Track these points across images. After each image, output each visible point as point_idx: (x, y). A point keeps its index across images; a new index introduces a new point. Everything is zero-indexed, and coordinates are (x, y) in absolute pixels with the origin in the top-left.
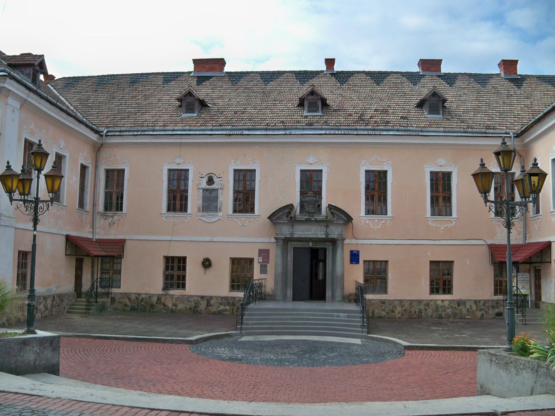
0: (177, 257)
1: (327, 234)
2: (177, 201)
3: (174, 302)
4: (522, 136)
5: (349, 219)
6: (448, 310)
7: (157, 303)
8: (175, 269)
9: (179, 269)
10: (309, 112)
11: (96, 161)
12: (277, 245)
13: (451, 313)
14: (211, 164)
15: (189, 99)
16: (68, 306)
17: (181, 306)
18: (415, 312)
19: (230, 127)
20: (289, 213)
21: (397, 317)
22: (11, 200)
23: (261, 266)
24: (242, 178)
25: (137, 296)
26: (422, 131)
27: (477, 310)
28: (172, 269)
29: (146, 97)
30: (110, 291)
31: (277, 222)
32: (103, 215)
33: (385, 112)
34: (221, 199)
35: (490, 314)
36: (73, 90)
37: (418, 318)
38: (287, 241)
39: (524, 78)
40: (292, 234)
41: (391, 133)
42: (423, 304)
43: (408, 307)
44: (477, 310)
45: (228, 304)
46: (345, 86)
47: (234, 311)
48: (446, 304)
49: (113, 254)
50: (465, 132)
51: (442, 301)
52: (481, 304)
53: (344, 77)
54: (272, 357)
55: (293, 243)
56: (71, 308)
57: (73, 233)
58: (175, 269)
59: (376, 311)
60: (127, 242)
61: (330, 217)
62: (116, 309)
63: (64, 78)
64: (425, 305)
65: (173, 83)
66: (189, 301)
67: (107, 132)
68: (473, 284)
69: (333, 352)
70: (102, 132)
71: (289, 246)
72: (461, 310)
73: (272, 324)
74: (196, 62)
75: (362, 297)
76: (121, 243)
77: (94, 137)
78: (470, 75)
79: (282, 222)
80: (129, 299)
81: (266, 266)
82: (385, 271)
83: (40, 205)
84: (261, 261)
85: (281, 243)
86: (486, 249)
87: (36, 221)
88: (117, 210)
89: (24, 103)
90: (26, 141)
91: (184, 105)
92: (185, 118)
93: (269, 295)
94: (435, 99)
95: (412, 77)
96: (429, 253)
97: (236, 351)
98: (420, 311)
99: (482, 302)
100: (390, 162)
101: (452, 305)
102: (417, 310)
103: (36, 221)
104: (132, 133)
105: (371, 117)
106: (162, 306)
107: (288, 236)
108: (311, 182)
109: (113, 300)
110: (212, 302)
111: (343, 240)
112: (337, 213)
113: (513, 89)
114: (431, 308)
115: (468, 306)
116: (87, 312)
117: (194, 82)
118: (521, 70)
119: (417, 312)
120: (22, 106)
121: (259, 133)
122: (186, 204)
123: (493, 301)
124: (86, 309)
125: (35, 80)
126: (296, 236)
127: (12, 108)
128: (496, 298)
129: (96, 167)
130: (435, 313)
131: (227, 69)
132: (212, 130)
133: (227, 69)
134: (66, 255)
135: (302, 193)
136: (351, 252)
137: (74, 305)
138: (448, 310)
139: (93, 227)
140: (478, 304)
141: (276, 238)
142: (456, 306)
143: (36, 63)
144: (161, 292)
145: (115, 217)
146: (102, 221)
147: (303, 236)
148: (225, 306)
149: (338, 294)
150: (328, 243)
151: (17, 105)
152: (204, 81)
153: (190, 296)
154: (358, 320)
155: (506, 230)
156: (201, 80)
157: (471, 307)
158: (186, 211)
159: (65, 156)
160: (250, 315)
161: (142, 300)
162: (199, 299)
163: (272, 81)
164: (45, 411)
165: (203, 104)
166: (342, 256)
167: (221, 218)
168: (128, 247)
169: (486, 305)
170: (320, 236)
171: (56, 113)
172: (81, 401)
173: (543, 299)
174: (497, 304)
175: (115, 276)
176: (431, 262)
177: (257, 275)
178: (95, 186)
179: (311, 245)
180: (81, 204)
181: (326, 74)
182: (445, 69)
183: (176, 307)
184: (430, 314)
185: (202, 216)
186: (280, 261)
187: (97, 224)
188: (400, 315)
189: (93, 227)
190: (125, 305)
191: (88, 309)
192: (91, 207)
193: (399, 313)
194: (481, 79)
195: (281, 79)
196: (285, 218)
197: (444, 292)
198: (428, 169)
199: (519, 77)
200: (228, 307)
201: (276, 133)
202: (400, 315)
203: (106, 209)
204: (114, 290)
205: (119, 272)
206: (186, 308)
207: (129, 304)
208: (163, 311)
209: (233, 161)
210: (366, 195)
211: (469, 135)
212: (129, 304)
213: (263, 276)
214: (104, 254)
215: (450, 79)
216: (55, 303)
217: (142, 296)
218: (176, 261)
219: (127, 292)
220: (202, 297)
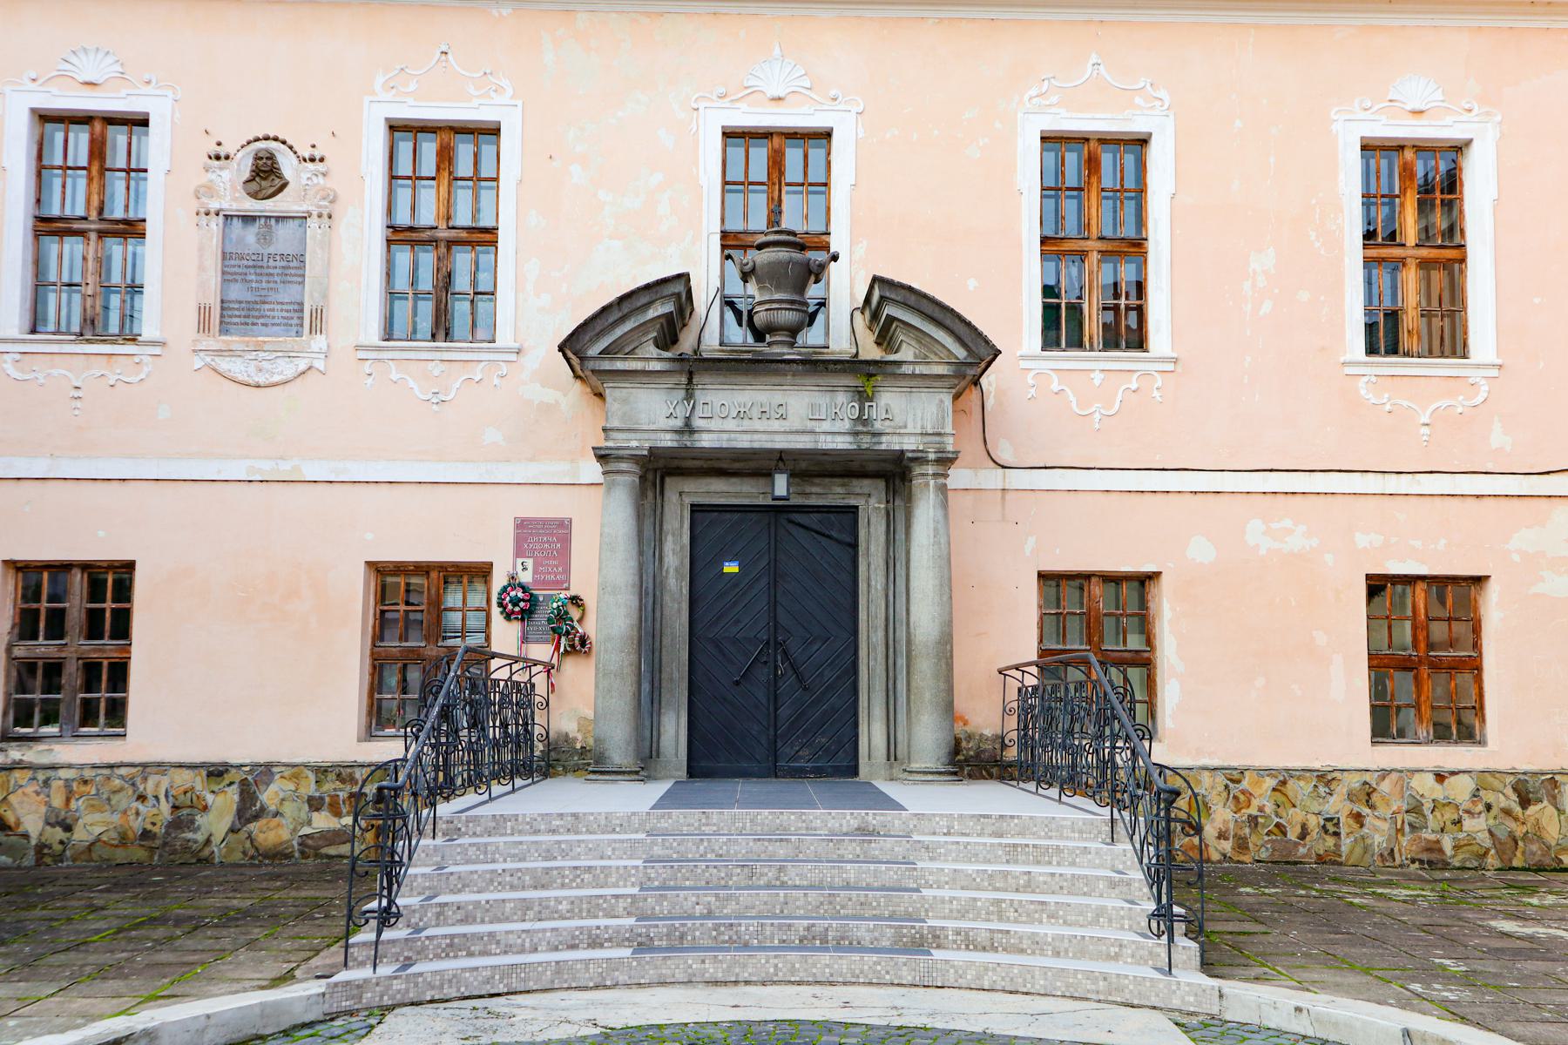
0: (86, 566)
3: (58, 801)
9: (94, 631)
17: (92, 825)
18: (1304, 834)
20: (669, 332)
21: (1215, 856)
31: (606, 365)
40: (688, 429)
42: (1341, 790)
48: (1461, 789)
51: (1440, 777)
64: (1351, 797)
66: (142, 798)
71: (671, 497)
79: (638, 365)
85: (628, 479)
100: (1162, 94)
101: (1488, 797)
102: (1314, 822)
107: (667, 441)
110: (269, 796)
111: (946, 461)
114: (1383, 811)
119: (1315, 832)
126: (706, 441)
130: (1404, 841)
138: (1469, 824)
141: (603, 457)
142: (1512, 802)
147: (744, 442)
150: (865, 485)
162: (198, 781)
167: (320, 364)
183: (68, 828)
185: (219, 352)
188: (1227, 846)
193: (1222, 836)
196: (652, 351)
197: (1441, 734)
202: (1227, 846)
209: (380, 80)
218: (78, 581)
220: (216, 772)
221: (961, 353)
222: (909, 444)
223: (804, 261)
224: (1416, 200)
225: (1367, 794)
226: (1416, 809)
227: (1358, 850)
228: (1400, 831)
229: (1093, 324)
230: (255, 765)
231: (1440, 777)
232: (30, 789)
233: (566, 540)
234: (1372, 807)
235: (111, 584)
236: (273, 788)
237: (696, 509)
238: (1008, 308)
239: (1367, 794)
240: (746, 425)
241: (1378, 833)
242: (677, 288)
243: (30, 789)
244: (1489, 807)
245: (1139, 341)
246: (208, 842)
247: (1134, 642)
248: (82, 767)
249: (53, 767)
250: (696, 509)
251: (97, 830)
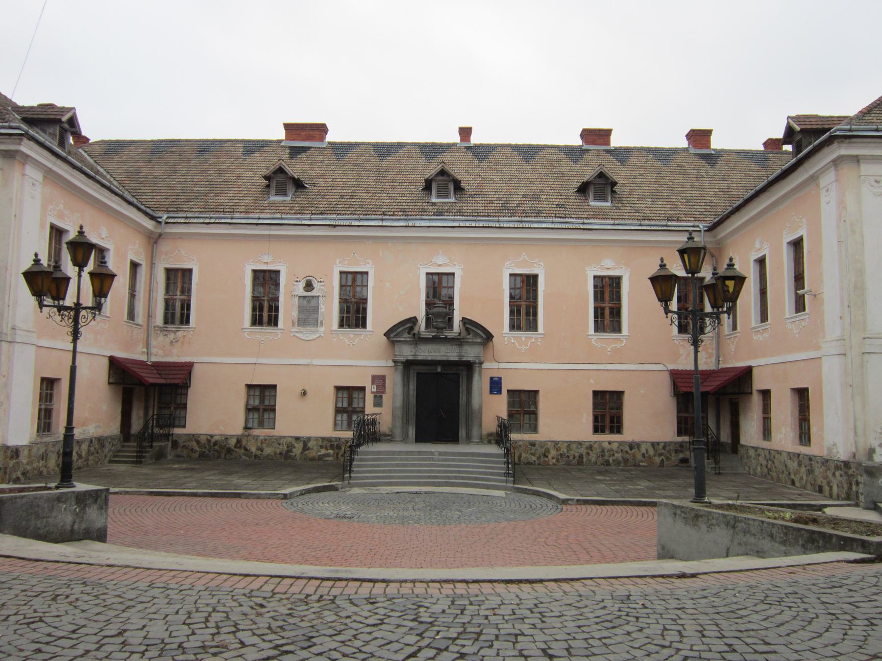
1: (460, 356)
2: (265, 312)
3: (259, 444)
4: (715, 231)
5: (489, 337)
6: (616, 455)
7: (235, 447)
8: (262, 399)
10: (438, 197)
11: (152, 257)
12: (396, 370)
13: (621, 459)
14: (310, 264)
15: (280, 178)
16: (111, 453)
17: (268, 451)
18: (574, 457)
19: (334, 216)
20: (412, 328)
22: (41, 305)
23: (375, 396)
24: (350, 283)
26: (584, 223)
27: (654, 455)
29: (220, 173)
32: (162, 329)
33: (536, 197)
34: (322, 308)
36: (116, 158)
37: (578, 464)
38: (408, 365)
39: (719, 153)
41: (544, 226)
43: (565, 451)
44: (654, 455)
45: (332, 447)
46: (484, 165)
47: (339, 456)
48: (615, 446)
49: (176, 381)
50: (641, 225)
51: (610, 443)
53: (483, 152)
54: (391, 514)
55: (416, 367)
56: (115, 456)
57: (120, 354)
58: (262, 399)
59: (524, 455)
60: (195, 365)
61: (464, 333)
62: (178, 456)
63: (103, 142)
65: (257, 154)
67: (168, 218)
68: (650, 420)
69: (469, 507)
70: (161, 218)
72: (634, 456)
73: (390, 471)
74: (288, 127)
75: (506, 436)
76: (187, 369)
77: (149, 224)
78: (648, 150)
80: (198, 442)
81: (381, 397)
82: (535, 404)
83: (83, 313)
84: (374, 390)
85: (401, 367)
86: (667, 375)
87: (76, 335)
88: (182, 323)
89: (49, 174)
90: (53, 227)
91: (274, 184)
92: (274, 202)
93: (386, 435)
94: (601, 181)
95: (570, 152)
96: (592, 381)
97: (343, 507)
98: (581, 456)
99: (662, 444)
103: (76, 335)
104: (202, 221)
105: (518, 205)
106: (243, 451)
107: (410, 358)
108: (439, 289)
109: (175, 444)
110: (310, 444)
111: (481, 363)
112: (474, 328)
113: (705, 168)
115: (643, 450)
116: (138, 461)
117: (286, 155)
118: (716, 143)
120: (45, 177)
121: (372, 223)
122: (276, 317)
123: (676, 443)
124: (137, 457)
125: (62, 143)
126: (420, 358)
127: (31, 181)
128: (680, 439)
129: (152, 265)
131: (330, 137)
132: (311, 219)
133: (330, 137)
134: (109, 383)
135: (429, 305)
136: (492, 378)
137: (119, 451)
138: (616, 455)
139: (148, 345)
140: (656, 447)
141: (395, 362)
142: (628, 449)
143: (64, 119)
145: (178, 333)
146: (161, 338)
147: (430, 358)
148: (327, 449)
149: (475, 433)
150: (461, 368)
151: (38, 176)
152: (300, 153)
153: (281, 437)
154: (500, 467)
155: (692, 347)
156: (295, 152)
157: (647, 450)
158: (276, 324)
159: (108, 250)
160: (361, 460)
161: (215, 443)
162: (293, 441)
163: (389, 155)
164: (101, 582)
165: (299, 184)
166: (480, 384)
168: (196, 372)
171: (95, 190)
172: (149, 569)
173: (742, 442)
175: (178, 412)
176: (596, 393)
177: (370, 408)
178: (150, 291)
179: (439, 370)
180: (131, 315)
181: (459, 148)
182: (616, 141)
184: (594, 459)
186: (399, 390)
187: (153, 343)
189: (148, 345)
191: (140, 457)
192: (146, 319)
193: (553, 458)
194: (662, 155)
195: (401, 153)
198: (591, 273)
199: (713, 152)
200: (331, 451)
201: (396, 224)
202: (554, 461)
203: (166, 322)
204: (177, 431)
205: (184, 406)
206: (275, 453)
207: (197, 448)
208: (244, 457)
209: (338, 261)
210: (510, 306)
211: (645, 228)
212: (197, 448)
213: (377, 410)
214: (162, 381)
215: (623, 154)
216: (92, 449)
217: (216, 438)
219: (194, 433)
220: (297, 439)
222: (471, 359)
225: (590, 447)
226: (603, 451)
233: (384, 381)
237: (418, 374)
238: (498, 320)
247: (532, 409)
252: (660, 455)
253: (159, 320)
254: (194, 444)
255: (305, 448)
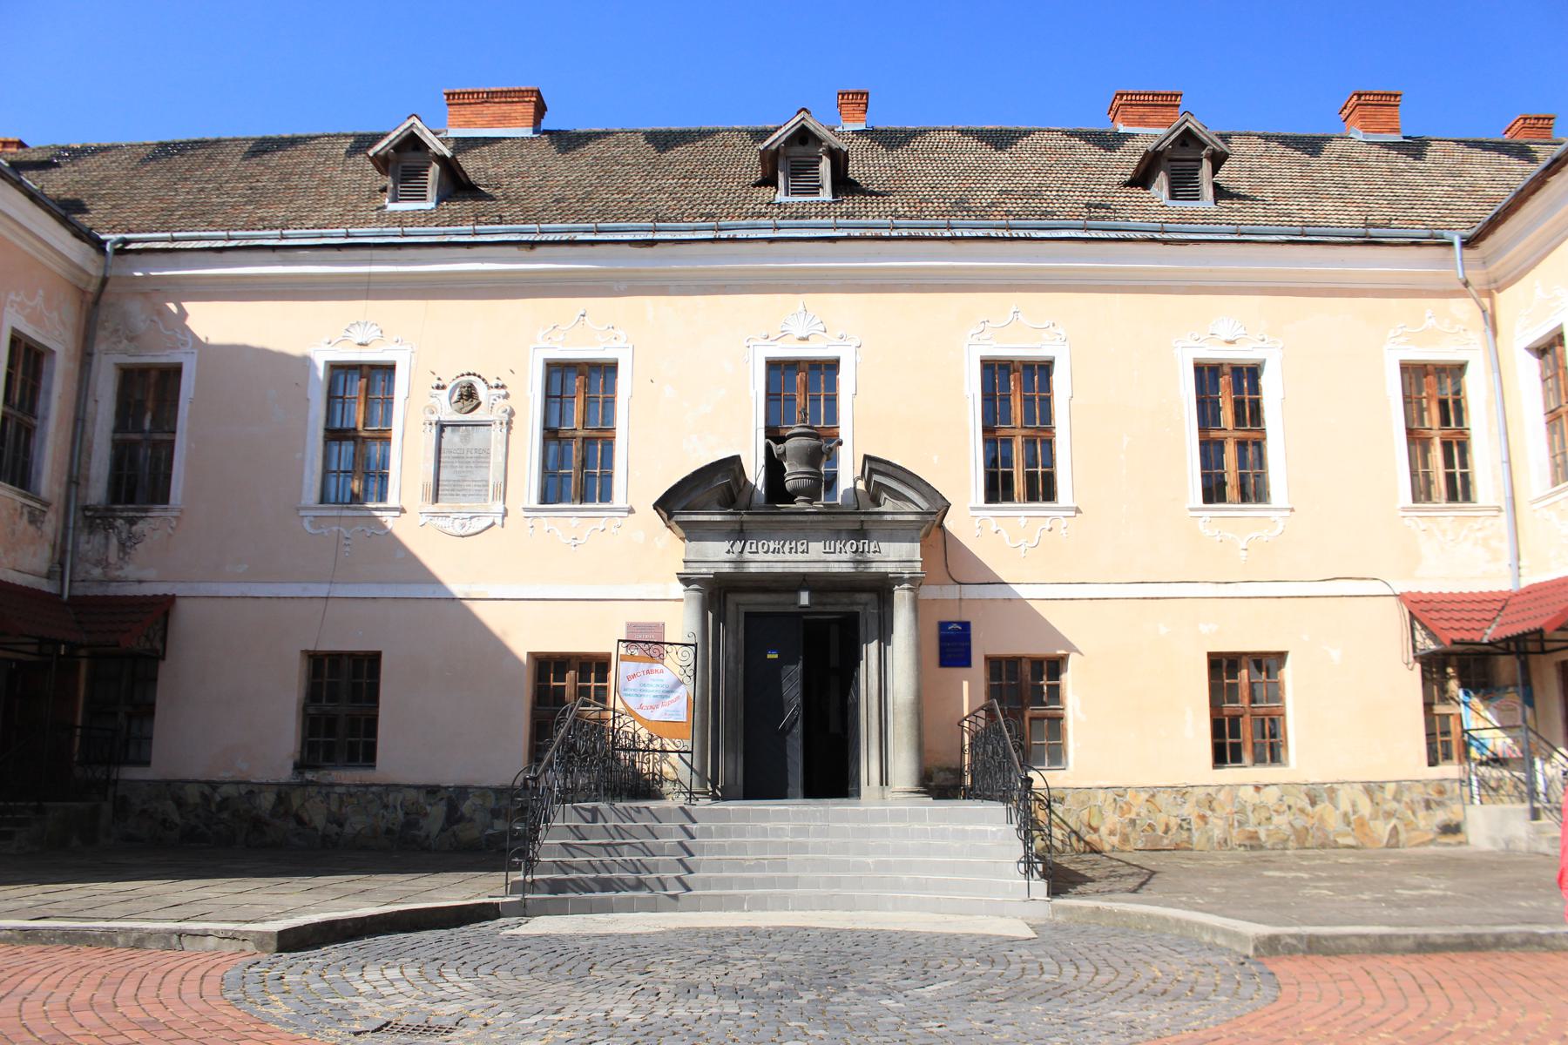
0: (352, 656)
3: (334, 808)
4: (1486, 245)
13: (1285, 827)
17: (357, 823)
21: (1107, 847)
25: (207, 790)
27: (1374, 817)
28: (332, 698)
30: (114, 776)
35: (1416, 829)
42: (1192, 800)
43: (1144, 812)
44: (1374, 817)
48: (1270, 796)
51: (1257, 788)
52: (1388, 794)
64: (1198, 804)
66: (386, 807)
69: (927, 980)
72: (1321, 819)
80: (180, 803)
99: (1391, 787)
101: (1289, 800)
102: (1174, 822)
106: (292, 825)
107: (726, 568)
110: (466, 807)
114: (1219, 812)
115: (1344, 805)
119: (1174, 829)
123: (1426, 784)
126: (753, 568)
130: (1235, 832)
136: (943, 626)
138: (1276, 819)
140: (1378, 796)
141: (686, 580)
142: (1305, 803)
144: (286, 774)
147: (778, 568)
150: (864, 597)
157: (1354, 805)
169: (1406, 798)
170: (836, 568)
174: (1441, 792)
183: (341, 825)
184: (1217, 834)
188: (1115, 840)
190: (165, 821)
193: (1112, 833)
197: (1258, 760)
202: (1115, 840)
212: (177, 818)
219: (170, 777)
220: (432, 791)
221: (925, 505)
223: (823, 449)
224: (1229, 399)
225: (1210, 802)
227: (1204, 840)
228: (1232, 825)
229: (1019, 485)
230: (457, 788)
231: (1257, 788)
232: (318, 799)
234: (1213, 810)
235: (369, 664)
236: (468, 803)
239: (1210, 802)
240: (780, 557)
241: (1217, 828)
242: (732, 465)
243: (318, 799)
244: (1290, 807)
245: (1050, 495)
246: (428, 837)
248: (348, 786)
249: (332, 785)
250: (747, 615)
251: (359, 827)
252: (1389, 815)
253: (97, 491)
254: (170, 806)
255: (453, 816)
